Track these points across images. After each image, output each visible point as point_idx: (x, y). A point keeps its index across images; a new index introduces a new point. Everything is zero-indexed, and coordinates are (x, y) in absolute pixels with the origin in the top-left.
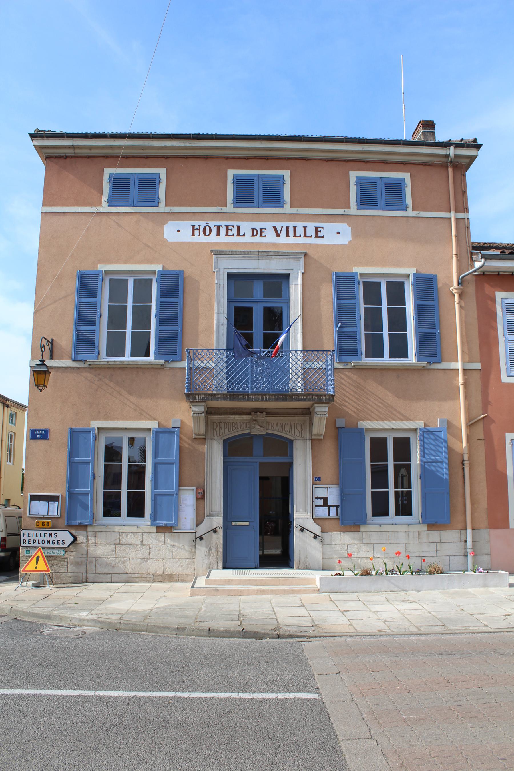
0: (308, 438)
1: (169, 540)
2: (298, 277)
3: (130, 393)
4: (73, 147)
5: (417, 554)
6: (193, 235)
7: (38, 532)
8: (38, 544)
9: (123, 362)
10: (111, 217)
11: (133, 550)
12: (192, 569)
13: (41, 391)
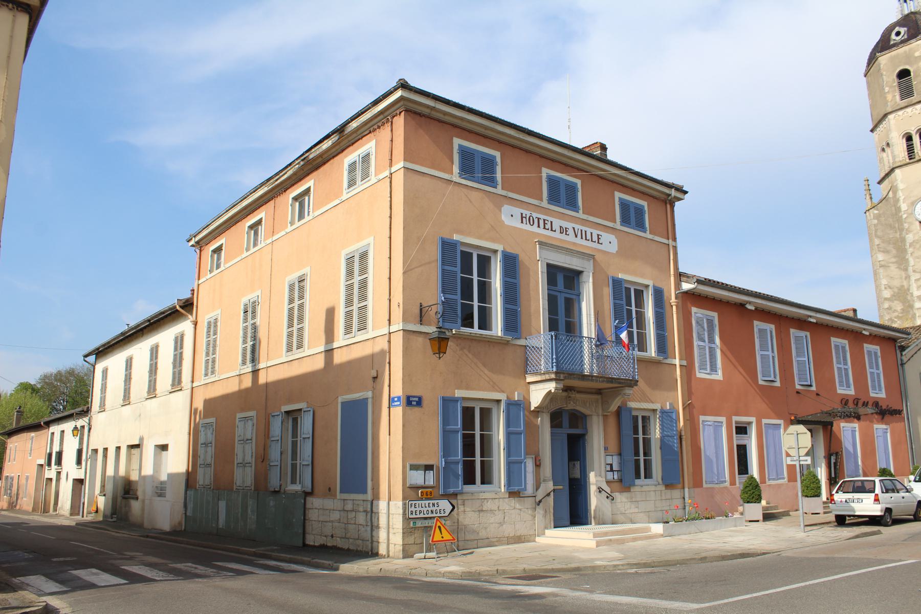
0: (600, 414)
1: (517, 505)
2: (589, 276)
3: (484, 365)
4: (433, 108)
5: (660, 509)
6: (522, 222)
7: (423, 502)
8: (424, 514)
9: (482, 335)
10: (461, 188)
11: (492, 515)
12: (534, 530)
13: (440, 358)
